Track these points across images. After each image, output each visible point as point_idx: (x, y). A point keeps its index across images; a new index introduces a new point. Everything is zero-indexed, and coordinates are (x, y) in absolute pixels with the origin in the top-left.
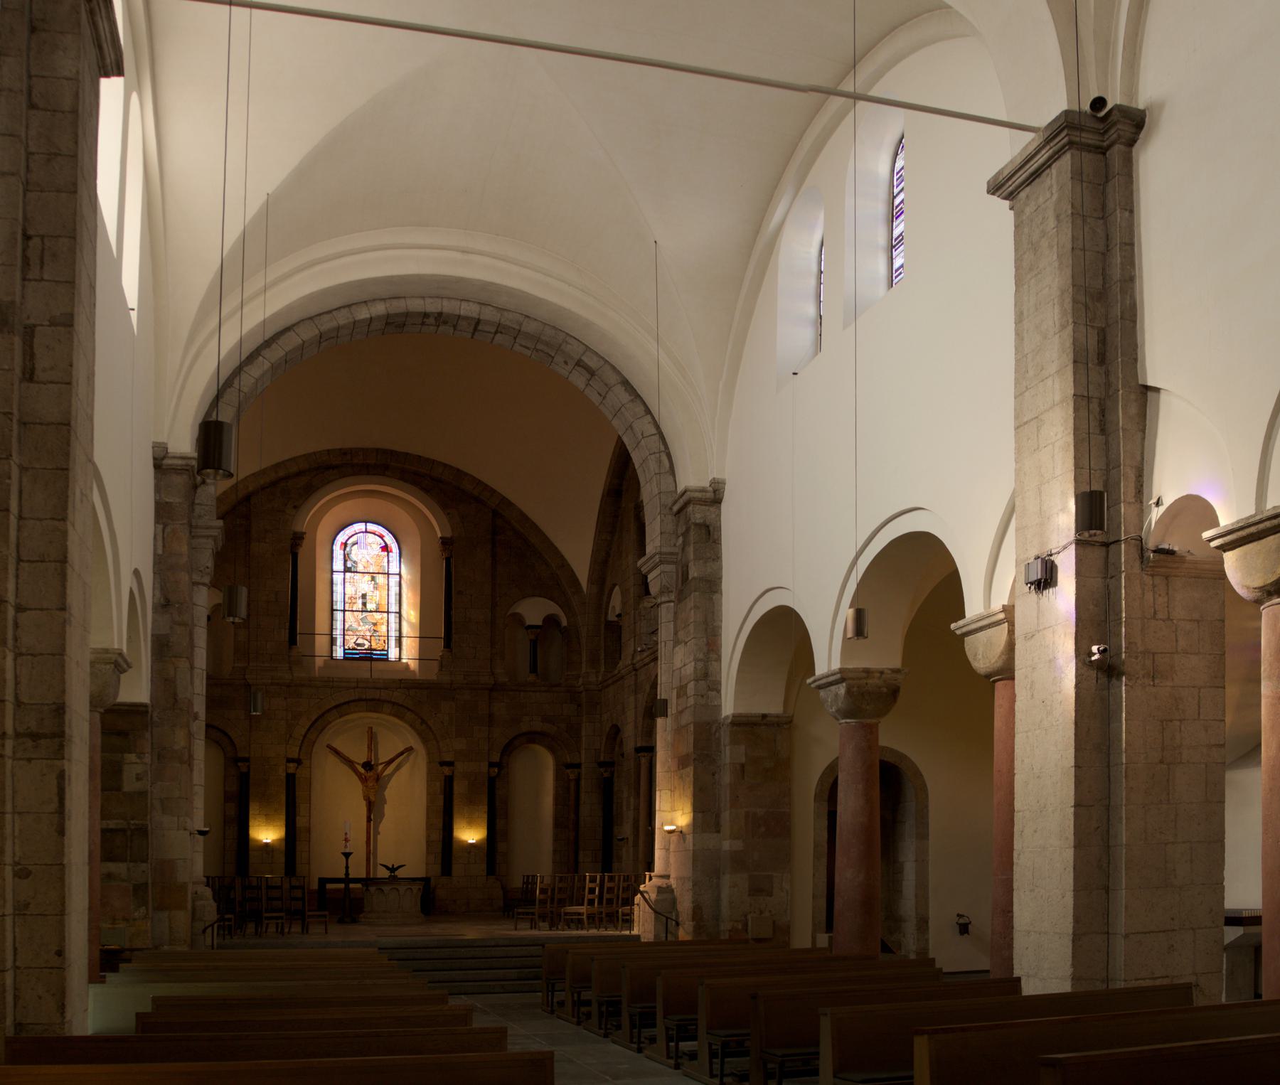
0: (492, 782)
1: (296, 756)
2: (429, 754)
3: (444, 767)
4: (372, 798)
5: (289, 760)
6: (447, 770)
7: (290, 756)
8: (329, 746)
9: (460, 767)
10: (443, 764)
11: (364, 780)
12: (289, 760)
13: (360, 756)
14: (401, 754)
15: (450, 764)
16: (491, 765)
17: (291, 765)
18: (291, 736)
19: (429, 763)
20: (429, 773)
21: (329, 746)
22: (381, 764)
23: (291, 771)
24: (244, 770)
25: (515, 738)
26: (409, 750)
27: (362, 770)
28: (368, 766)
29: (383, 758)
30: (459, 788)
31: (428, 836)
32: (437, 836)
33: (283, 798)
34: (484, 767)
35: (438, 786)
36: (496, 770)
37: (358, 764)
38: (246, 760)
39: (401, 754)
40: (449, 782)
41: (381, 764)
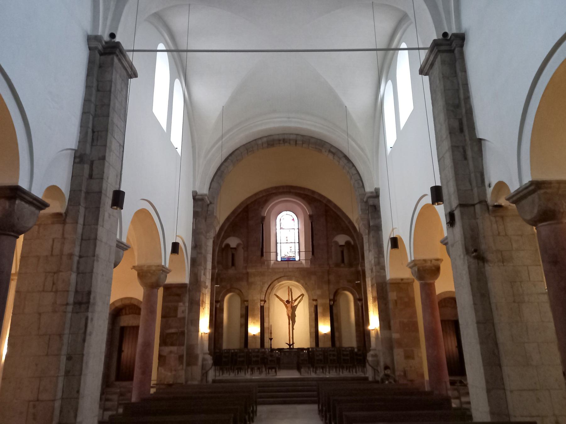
0: (331, 308)
1: (264, 299)
2: (309, 296)
5: (261, 301)
6: (315, 303)
8: (275, 295)
9: (320, 301)
10: (314, 300)
11: (287, 307)
12: (261, 301)
13: (286, 299)
14: (299, 297)
15: (316, 300)
16: (330, 300)
19: (309, 299)
20: (310, 304)
21: (275, 295)
23: (261, 305)
24: (246, 305)
26: (303, 295)
28: (288, 302)
29: (294, 299)
30: (320, 310)
31: (310, 330)
32: (313, 330)
33: (260, 316)
34: (328, 302)
35: (313, 309)
36: (332, 303)
38: (247, 301)
39: (299, 297)
40: (316, 307)
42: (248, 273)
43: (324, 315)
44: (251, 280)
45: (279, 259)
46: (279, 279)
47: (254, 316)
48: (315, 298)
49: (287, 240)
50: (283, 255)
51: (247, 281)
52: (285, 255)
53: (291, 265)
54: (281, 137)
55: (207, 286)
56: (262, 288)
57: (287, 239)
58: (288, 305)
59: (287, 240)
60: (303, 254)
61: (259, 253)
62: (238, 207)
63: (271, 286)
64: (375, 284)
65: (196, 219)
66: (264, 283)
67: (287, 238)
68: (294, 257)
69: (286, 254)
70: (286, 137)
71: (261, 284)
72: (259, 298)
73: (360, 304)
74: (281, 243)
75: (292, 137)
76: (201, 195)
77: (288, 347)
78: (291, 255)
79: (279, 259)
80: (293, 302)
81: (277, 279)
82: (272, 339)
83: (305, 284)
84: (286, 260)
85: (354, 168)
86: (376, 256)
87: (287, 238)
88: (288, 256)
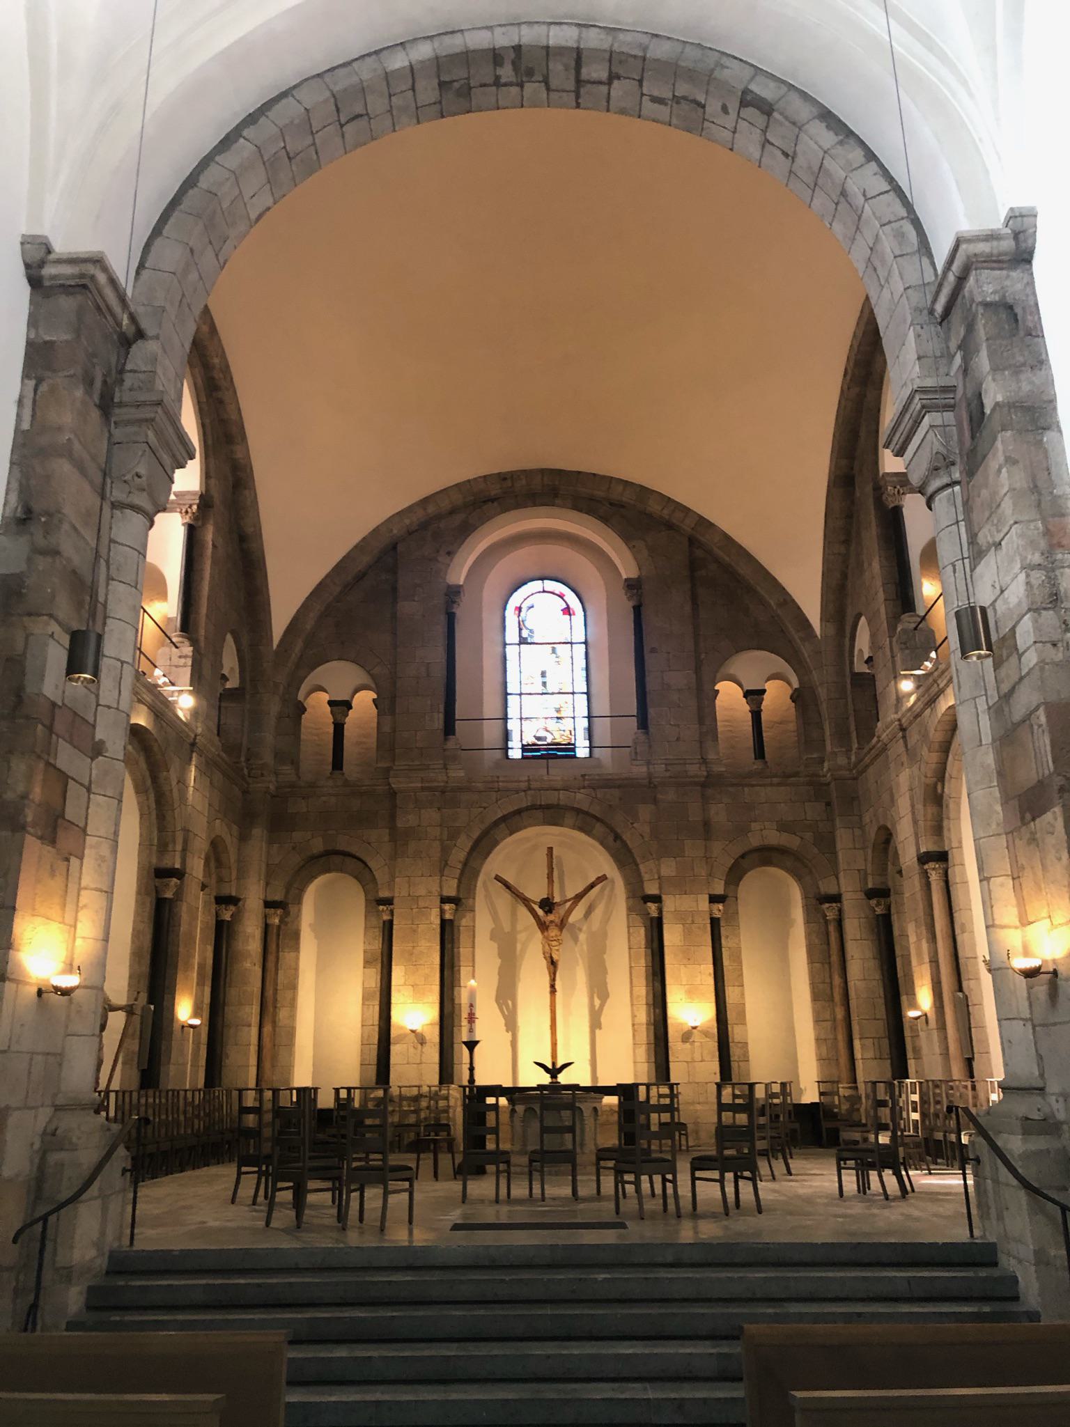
0: (715, 923)
1: (452, 893)
3: (649, 904)
4: (555, 957)
5: (444, 900)
6: (652, 907)
7: (445, 894)
8: (498, 878)
9: (670, 904)
13: (536, 892)
14: (592, 886)
15: (657, 899)
16: (714, 899)
17: (447, 907)
18: (446, 864)
21: (498, 878)
22: (569, 900)
23: (448, 916)
25: (743, 856)
26: (602, 878)
27: (540, 912)
28: (547, 905)
34: (704, 904)
37: (535, 903)
41: (569, 900)
42: (393, 794)
43: (688, 958)
44: (406, 820)
45: (515, 754)
46: (512, 821)
47: (413, 961)
48: (652, 889)
49: (544, 684)
50: (529, 739)
51: (393, 828)
52: (538, 739)
53: (558, 772)
54: (503, 39)
55: (102, 742)
56: (445, 851)
57: (544, 680)
58: (551, 917)
59: (544, 684)
60: (603, 726)
61: (438, 721)
62: (360, 547)
63: (483, 846)
64: (1041, 712)
65: (39, 381)
66: (454, 835)
67: (543, 674)
68: (569, 744)
69: (542, 734)
70: (528, 36)
71: (445, 837)
72: (435, 888)
73: (830, 912)
74: (521, 694)
75: (562, 37)
76: (72, 261)
77: (546, 1079)
78: (556, 734)
79: (515, 754)
80: (568, 904)
81: (504, 819)
82: (477, 1042)
83: (611, 838)
84: (541, 757)
85: (873, 164)
86: (1037, 558)
87: (543, 674)
88: (549, 741)
